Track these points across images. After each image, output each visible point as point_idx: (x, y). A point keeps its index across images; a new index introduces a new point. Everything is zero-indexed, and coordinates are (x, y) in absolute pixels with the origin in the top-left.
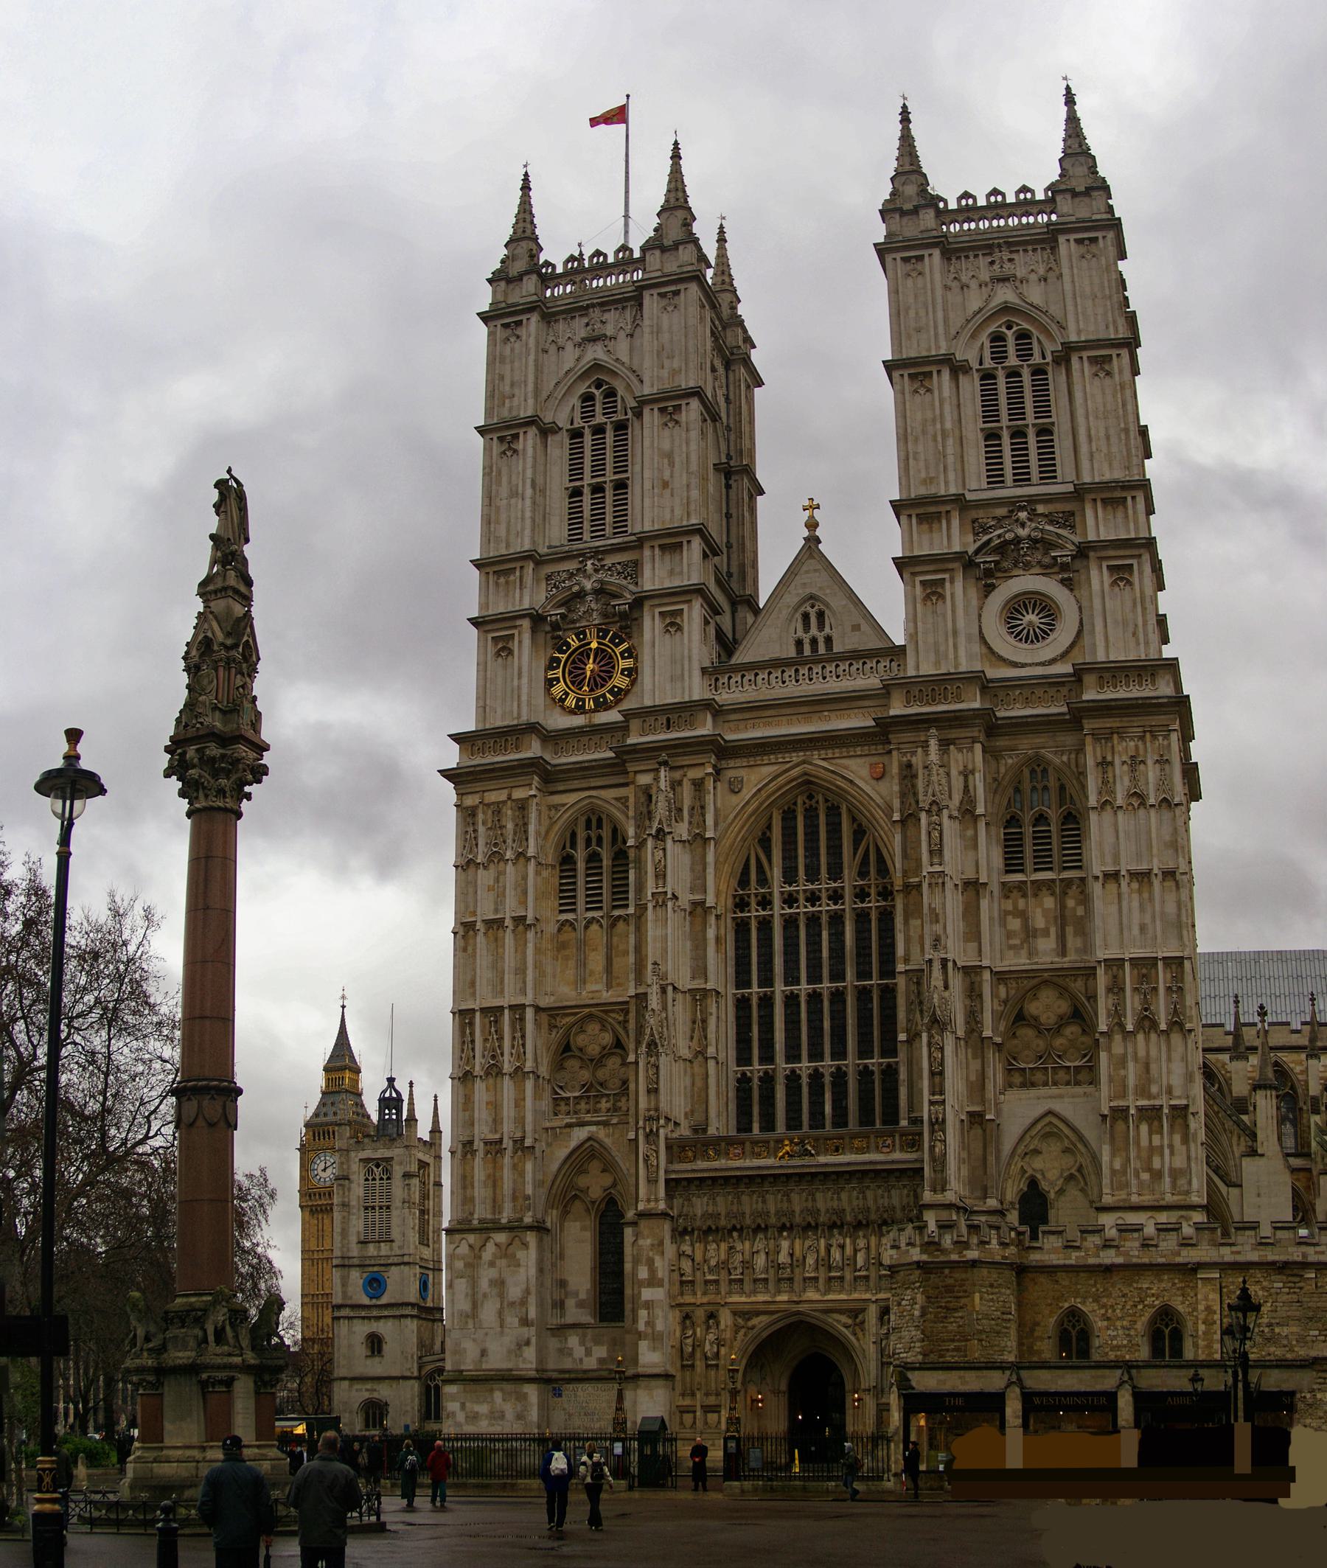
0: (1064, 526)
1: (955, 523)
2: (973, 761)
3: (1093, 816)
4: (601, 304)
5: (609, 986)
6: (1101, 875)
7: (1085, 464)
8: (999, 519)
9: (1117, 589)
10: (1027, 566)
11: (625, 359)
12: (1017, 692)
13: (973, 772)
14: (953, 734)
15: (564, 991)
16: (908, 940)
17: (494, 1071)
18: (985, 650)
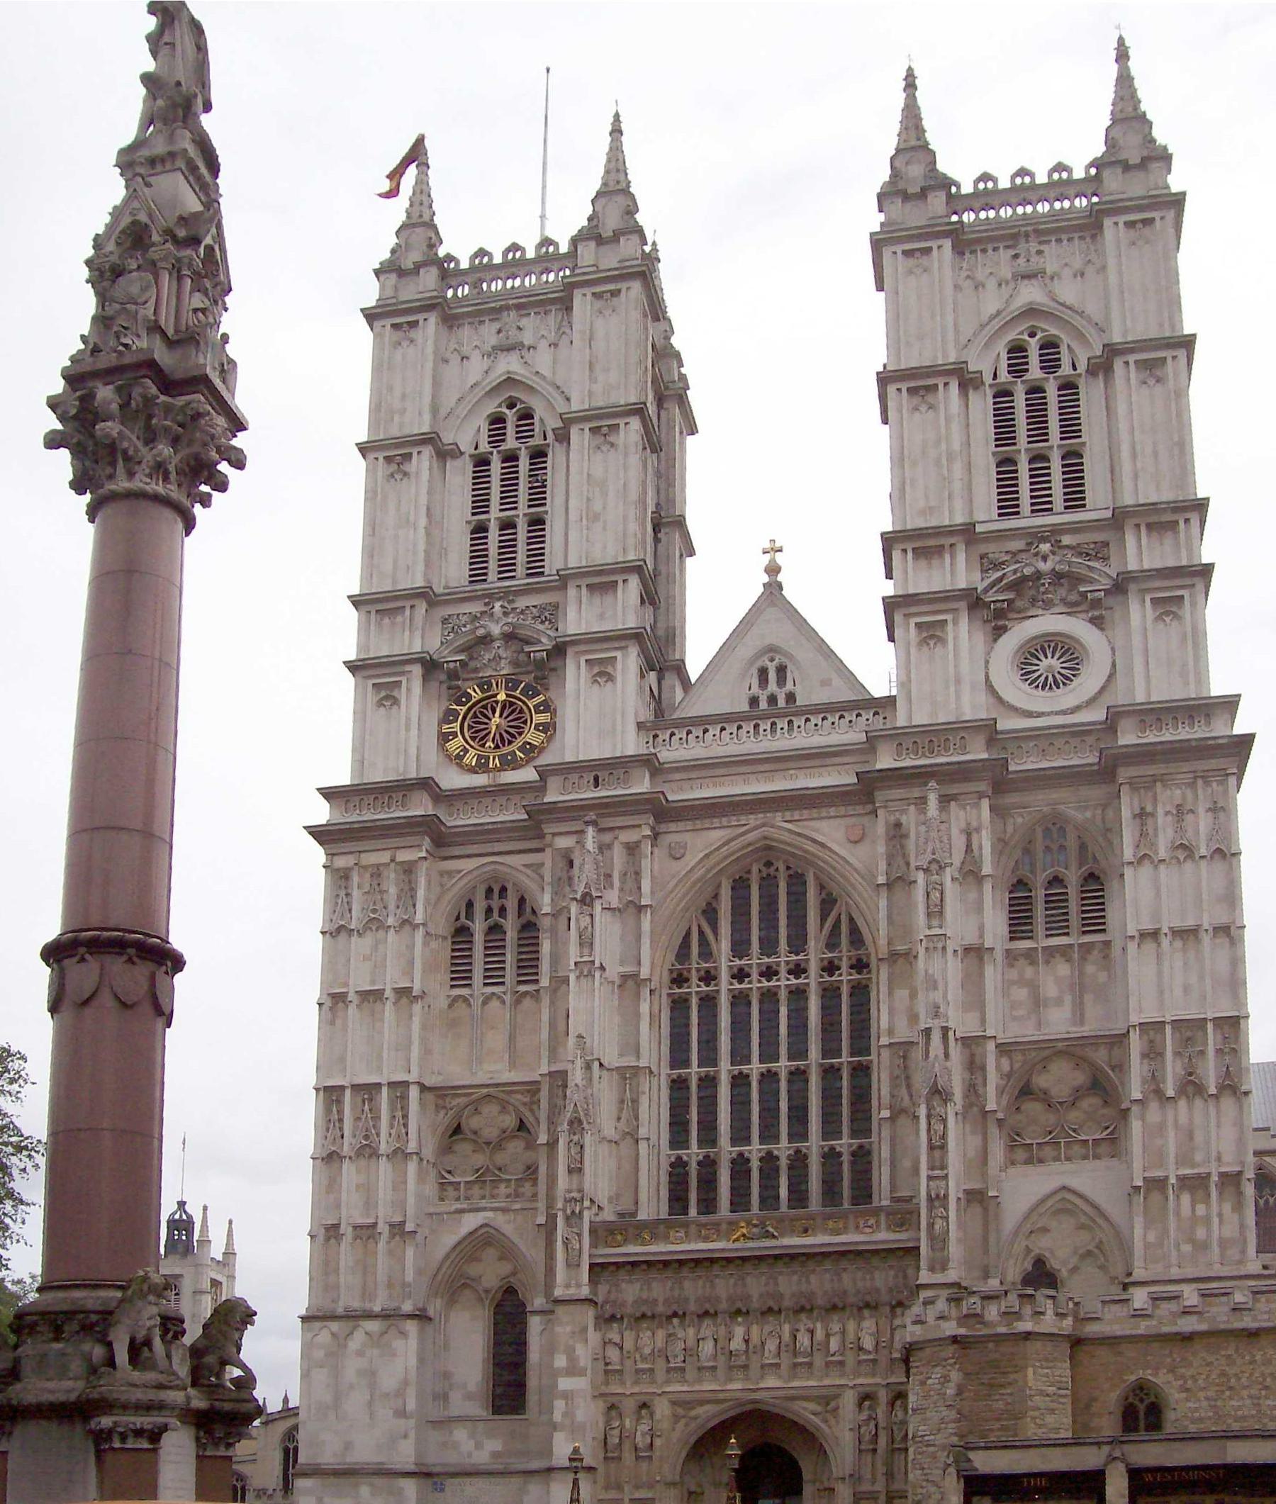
0: (1097, 558)
1: (961, 557)
2: (979, 817)
3: (1128, 872)
4: (519, 307)
5: (513, 1065)
6: (1137, 934)
7: (1127, 483)
8: (1014, 554)
9: (1161, 626)
10: (1048, 605)
11: (546, 372)
12: (1032, 744)
13: (978, 830)
14: (954, 789)
15: (456, 1071)
16: (891, 1012)
17: (368, 1151)
18: (992, 700)
